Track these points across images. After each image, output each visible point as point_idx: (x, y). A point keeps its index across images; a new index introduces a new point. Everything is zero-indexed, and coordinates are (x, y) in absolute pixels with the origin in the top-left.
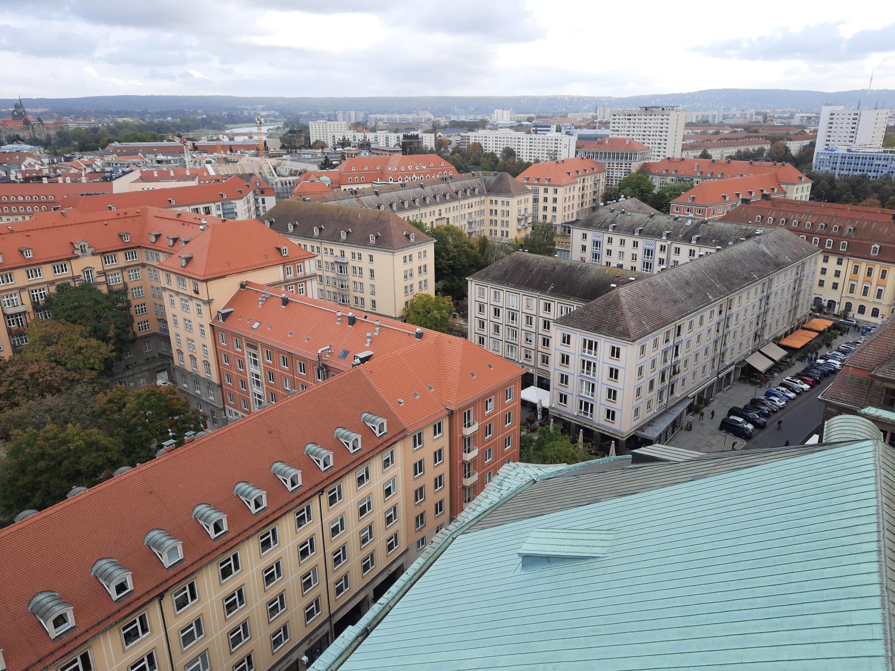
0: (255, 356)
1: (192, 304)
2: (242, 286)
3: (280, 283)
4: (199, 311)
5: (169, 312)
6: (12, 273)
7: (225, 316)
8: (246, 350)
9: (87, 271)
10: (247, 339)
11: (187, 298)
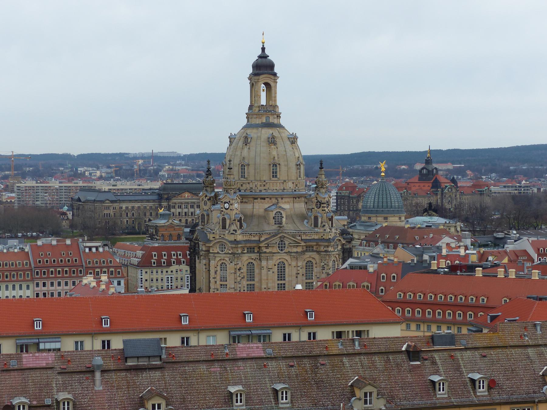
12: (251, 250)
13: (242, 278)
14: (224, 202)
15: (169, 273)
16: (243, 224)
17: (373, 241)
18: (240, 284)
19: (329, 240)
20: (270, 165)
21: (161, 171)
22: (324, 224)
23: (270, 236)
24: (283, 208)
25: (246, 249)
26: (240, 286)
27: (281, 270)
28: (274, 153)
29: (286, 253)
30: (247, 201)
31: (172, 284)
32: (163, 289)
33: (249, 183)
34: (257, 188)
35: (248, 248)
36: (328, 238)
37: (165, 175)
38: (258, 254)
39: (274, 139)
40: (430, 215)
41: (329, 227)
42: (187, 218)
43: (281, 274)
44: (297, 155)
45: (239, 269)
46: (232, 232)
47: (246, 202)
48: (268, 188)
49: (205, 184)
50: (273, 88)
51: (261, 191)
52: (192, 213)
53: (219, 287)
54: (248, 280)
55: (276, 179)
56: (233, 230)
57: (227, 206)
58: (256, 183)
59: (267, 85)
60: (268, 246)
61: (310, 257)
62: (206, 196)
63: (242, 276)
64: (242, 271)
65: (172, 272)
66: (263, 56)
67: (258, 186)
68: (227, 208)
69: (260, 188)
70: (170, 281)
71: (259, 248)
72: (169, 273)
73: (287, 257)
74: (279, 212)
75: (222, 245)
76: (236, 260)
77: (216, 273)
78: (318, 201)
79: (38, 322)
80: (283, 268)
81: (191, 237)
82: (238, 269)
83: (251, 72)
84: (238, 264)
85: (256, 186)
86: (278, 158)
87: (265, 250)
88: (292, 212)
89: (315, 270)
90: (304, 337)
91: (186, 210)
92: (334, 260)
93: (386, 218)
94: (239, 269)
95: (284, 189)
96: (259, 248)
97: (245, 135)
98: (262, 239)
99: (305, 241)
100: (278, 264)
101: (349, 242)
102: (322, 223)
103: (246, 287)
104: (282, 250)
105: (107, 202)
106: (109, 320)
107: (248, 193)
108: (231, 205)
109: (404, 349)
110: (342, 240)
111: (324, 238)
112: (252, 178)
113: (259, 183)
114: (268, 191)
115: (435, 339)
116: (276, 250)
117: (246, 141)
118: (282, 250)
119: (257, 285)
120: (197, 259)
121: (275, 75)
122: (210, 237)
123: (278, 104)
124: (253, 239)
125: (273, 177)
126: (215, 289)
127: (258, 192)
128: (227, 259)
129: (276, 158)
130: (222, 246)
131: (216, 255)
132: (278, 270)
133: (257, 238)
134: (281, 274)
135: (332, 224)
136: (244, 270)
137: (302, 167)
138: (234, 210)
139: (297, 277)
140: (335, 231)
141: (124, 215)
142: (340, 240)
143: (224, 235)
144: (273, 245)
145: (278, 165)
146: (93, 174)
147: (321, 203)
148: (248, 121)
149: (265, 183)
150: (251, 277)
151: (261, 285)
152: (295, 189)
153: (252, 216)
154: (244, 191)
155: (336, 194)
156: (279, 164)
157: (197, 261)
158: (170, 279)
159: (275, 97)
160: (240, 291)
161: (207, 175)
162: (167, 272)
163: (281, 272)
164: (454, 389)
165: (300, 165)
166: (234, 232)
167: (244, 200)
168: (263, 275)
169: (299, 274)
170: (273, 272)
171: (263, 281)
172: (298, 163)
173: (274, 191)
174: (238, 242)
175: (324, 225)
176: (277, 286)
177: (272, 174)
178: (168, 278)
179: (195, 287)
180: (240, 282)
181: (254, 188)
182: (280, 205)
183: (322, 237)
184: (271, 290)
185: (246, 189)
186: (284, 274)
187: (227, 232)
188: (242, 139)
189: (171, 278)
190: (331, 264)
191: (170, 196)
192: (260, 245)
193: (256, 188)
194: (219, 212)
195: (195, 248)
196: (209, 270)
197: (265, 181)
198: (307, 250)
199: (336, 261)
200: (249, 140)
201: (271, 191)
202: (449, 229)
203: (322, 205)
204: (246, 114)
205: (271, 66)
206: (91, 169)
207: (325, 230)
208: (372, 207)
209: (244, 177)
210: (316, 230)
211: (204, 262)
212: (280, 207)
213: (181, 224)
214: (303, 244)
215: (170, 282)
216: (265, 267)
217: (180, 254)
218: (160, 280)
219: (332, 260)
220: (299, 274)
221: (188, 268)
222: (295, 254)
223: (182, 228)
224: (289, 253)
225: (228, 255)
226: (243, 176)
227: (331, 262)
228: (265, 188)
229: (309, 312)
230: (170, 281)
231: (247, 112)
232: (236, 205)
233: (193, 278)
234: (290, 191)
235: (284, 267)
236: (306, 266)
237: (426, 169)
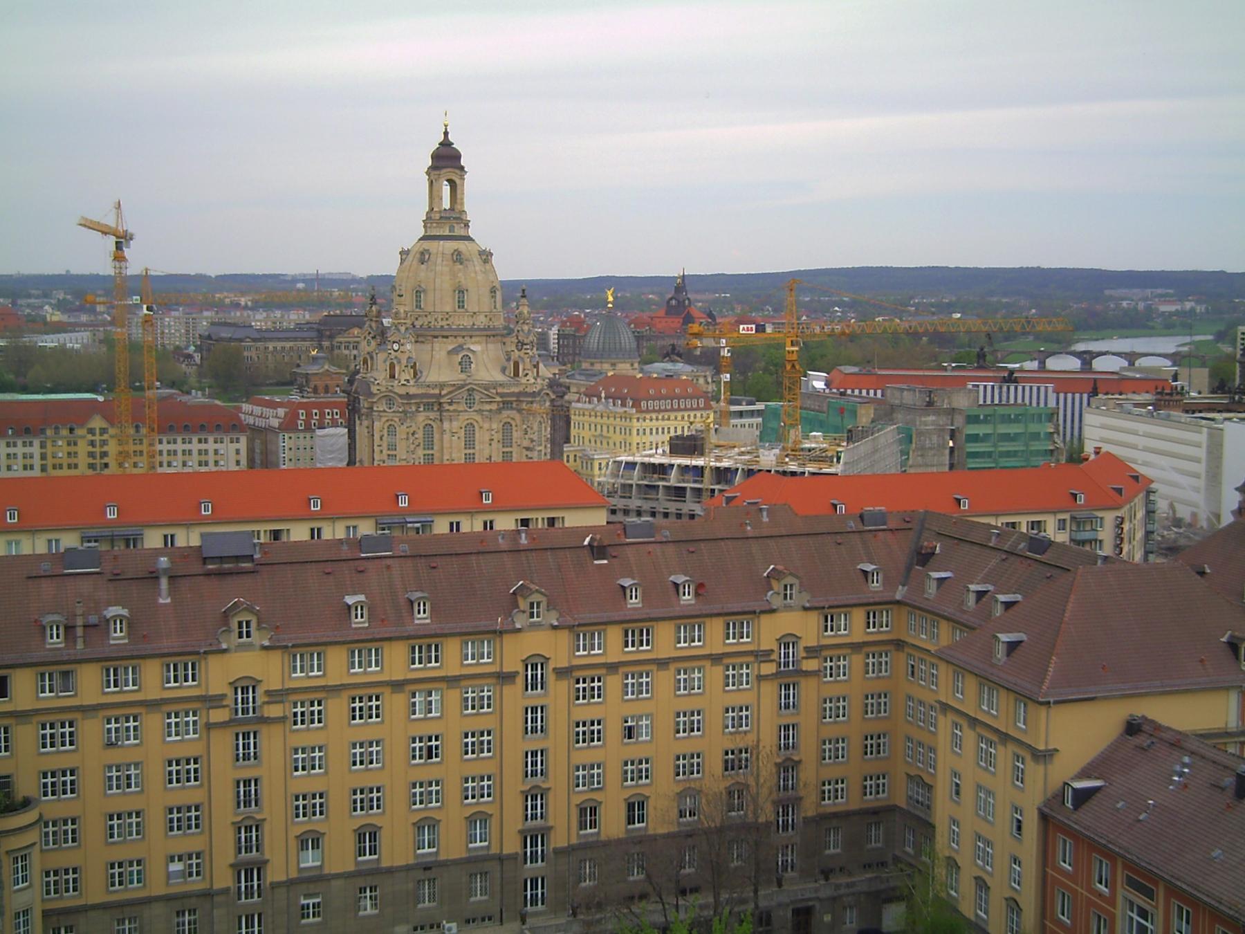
0: (1143, 914)
1: (1004, 755)
2: (1133, 728)
3: (1228, 734)
4: (1019, 776)
5: (945, 759)
6: (653, 627)
7: (1083, 797)
8: (1124, 892)
9: (788, 641)
10: (1129, 865)
11: (995, 738)
12: (428, 407)
17: (595, 396)
19: (533, 394)
20: (455, 291)
22: (526, 372)
23: (454, 388)
25: (422, 406)
26: (414, 456)
29: (476, 411)
30: (423, 340)
33: (426, 316)
35: (424, 405)
38: (438, 413)
40: (672, 361)
45: (413, 434)
46: (403, 382)
47: (423, 342)
50: (458, 187)
53: (385, 458)
54: (424, 449)
55: (462, 310)
57: (396, 347)
59: (452, 183)
60: (452, 402)
61: (508, 417)
62: (370, 333)
64: (416, 436)
66: (446, 143)
67: (439, 320)
71: (440, 404)
73: (478, 418)
74: (467, 356)
75: (390, 400)
76: (408, 421)
77: (381, 439)
78: (519, 342)
79: (12, 512)
81: (349, 389)
83: (430, 164)
85: (436, 320)
87: (447, 407)
89: (515, 434)
90: (479, 527)
93: (613, 365)
94: (413, 434)
96: (440, 404)
98: (443, 392)
99: (502, 395)
101: (562, 397)
102: (524, 370)
103: (422, 457)
104: (470, 408)
106: (16, 513)
108: (402, 345)
109: (586, 543)
110: (550, 393)
117: (424, 257)
119: (437, 455)
121: (462, 168)
122: (374, 389)
123: (466, 209)
124: (432, 392)
125: (459, 307)
126: (380, 461)
128: (397, 420)
130: (390, 401)
131: (382, 414)
133: (437, 391)
135: (538, 372)
136: (420, 435)
139: (490, 445)
142: (548, 394)
147: (523, 344)
148: (426, 232)
149: (447, 316)
150: (429, 444)
151: (443, 455)
157: (358, 422)
159: (462, 199)
165: (495, 292)
166: (405, 383)
167: (420, 339)
168: (445, 441)
169: (492, 440)
170: (459, 438)
171: (445, 451)
174: (410, 396)
175: (527, 374)
176: (463, 456)
184: (456, 462)
186: (474, 441)
187: (396, 382)
188: (418, 256)
190: (536, 427)
192: (442, 401)
194: (387, 355)
195: (354, 405)
196: (373, 435)
198: (504, 408)
200: (427, 257)
202: (697, 380)
203: (525, 347)
204: (424, 221)
205: (457, 156)
208: (595, 349)
209: (420, 308)
211: (365, 423)
212: (469, 349)
214: (498, 399)
216: (448, 431)
220: (492, 440)
224: (480, 411)
225: (399, 415)
226: (418, 306)
232: (408, 347)
233: (352, 446)
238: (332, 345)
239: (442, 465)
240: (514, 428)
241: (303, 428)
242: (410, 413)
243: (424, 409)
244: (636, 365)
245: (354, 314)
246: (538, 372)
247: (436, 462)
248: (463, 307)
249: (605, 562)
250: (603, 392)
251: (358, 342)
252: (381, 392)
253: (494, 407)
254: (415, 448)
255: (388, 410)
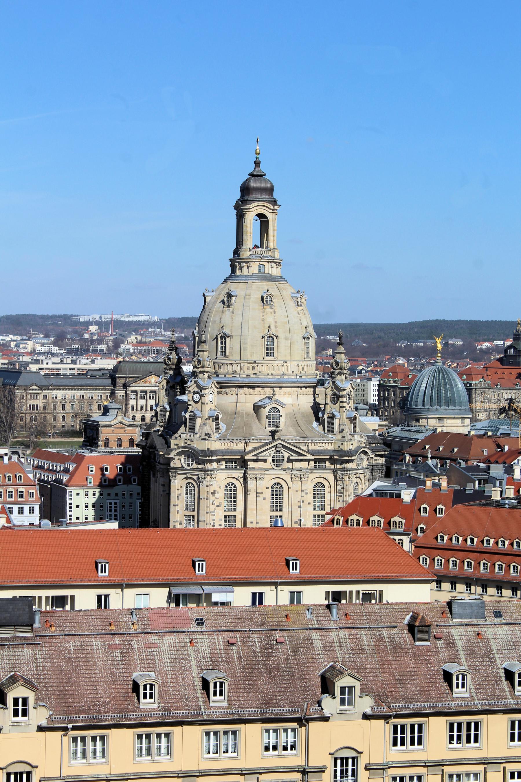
13: (218, 506)
14: (192, 391)
15: (113, 495)
16: (221, 426)
18: (214, 515)
21: (123, 343)
22: (342, 427)
23: (261, 444)
24: (281, 403)
25: (224, 463)
26: (214, 517)
27: (277, 495)
28: (270, 319)
31: (116, 513)
32: (89, 520)
34: (244, 372)
36: (348, 449)
37: (129, 349)
39: (270, 298)
41: (349, 433)
42: (134, 415)
43: (277, 502)
44: (305, 324)
45: (214, 493)
46: (203, 436)
48: (260, 372)
49: (166, 364)
51: (248, 376)
52: (142, 408)
55: (272, 358)
56: (206, 435)
58: (242, 365)
63: (217, 503)
64: (216, 495)
65: (116, 494)
67: (245, 368)
68: (198, 400)
69: (247, 372)
70: (113, 509)
72: (113, 495)
80: (279, 493)
82: (212, 493)
84: (212, 485)
85: (241, 369)
86: (276, 327)
88: (295, 409)
91: (142, 402)
92: (356, 482)
94: (214, 493)
95: (284, 374)
97: (227, 291)
100: (272, 487)
103: (223, 519)
105: (34, 387)
107: (229, 378)
110: (369, 452)
111: (341, 449)
112: (236, 357)
113: (247, 365)
114: (260, 377)
115: (455, 608)
116: (269, 465)
118: (278, 466)
120: (151, 476)
121: (275, 202)
125: (268, 355)
127: (244, 378)
129: (272, 327)
132: (272, 495)
134: (277, 502)
135: (355, 428)
137: (312, 343)
138: (207, 404)
140: (360, 439)
141: (59, 408)
143: (192, 441)
144: (265, 458)
145: (275, 338)
146: (21, 346)
152: (300, 375)
153: (235, 414)
154: (223, 376)
155: (378, 383)
156: (277, 337)
157: (152, 479)
158: (113, 505)
160: (214, 526)
161: (170, 350)
162: (109, 494)
163: (277, 498)
164: (479, 685)
166: (207, 437)
167: (223, 390)
170: (264, 499)
172: (306, 336)
173: (269, 377)
175: (343, 430)
177: (266, 352)
178: (110, 503)
179: (149, 518)
180: (214, 512)
181: (238, 372)
182: (276, 397)
183: (339, 447)
185: (227, 373)
189: (115, 503)
191: (129, 381)
193: (242, 372)
197: (255, 362)
199: (359, 484)
201: (263, 377)
204: (231, 260)
206: (18, 338)
207: (344, 437)
210: (330, 436)
213: (136, 423)
214: (310, 457)
215: (113, 511)
217: (129, 469)
218: (127, 505)
219: (354, 482)
221: (139, 489)
222: (298, 472)
223: (137, 429)
227: (353, 485)
228: (255, 371)
229: (291, 560)
230: (113, 509)
231: (232, 257)
234: (293, 377)
235: (281, 491)
236: (315, 490)
237: (515, 348)
238: (126, 393)
239: (288, 528)
240: (327, 490)
241: (92, 484)
242: (211, 470)
243: (227, 466)
244: (468, 422)
245: (152, 360)
246: (355, 428)
247: (239, 525)
248: (273, 355)
249: (428, 643)
250: (430, 451)
251: (155, 392)
252: (179, 448)
253: (304, 465)
254: (215, 509)
255: (186, 467)
